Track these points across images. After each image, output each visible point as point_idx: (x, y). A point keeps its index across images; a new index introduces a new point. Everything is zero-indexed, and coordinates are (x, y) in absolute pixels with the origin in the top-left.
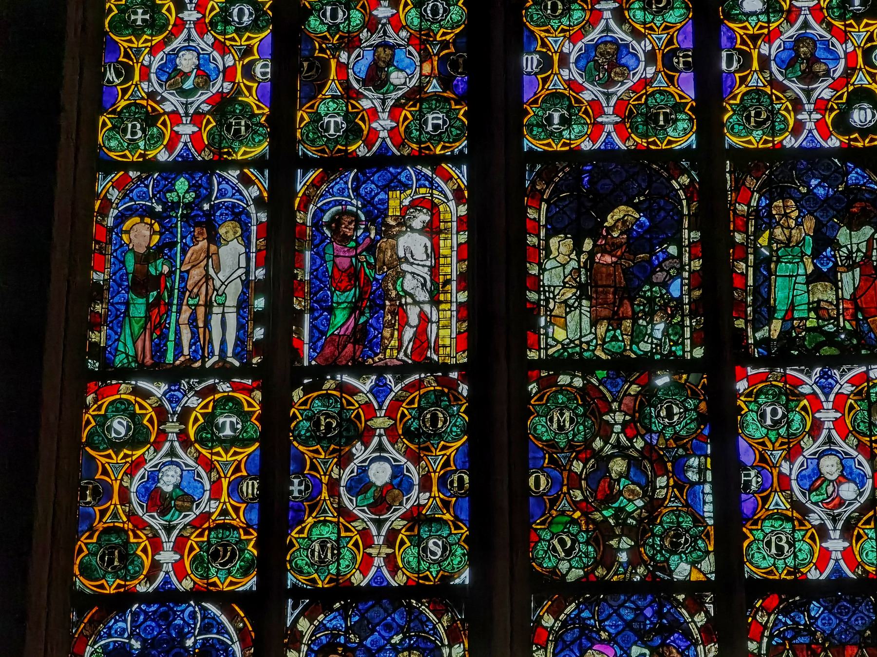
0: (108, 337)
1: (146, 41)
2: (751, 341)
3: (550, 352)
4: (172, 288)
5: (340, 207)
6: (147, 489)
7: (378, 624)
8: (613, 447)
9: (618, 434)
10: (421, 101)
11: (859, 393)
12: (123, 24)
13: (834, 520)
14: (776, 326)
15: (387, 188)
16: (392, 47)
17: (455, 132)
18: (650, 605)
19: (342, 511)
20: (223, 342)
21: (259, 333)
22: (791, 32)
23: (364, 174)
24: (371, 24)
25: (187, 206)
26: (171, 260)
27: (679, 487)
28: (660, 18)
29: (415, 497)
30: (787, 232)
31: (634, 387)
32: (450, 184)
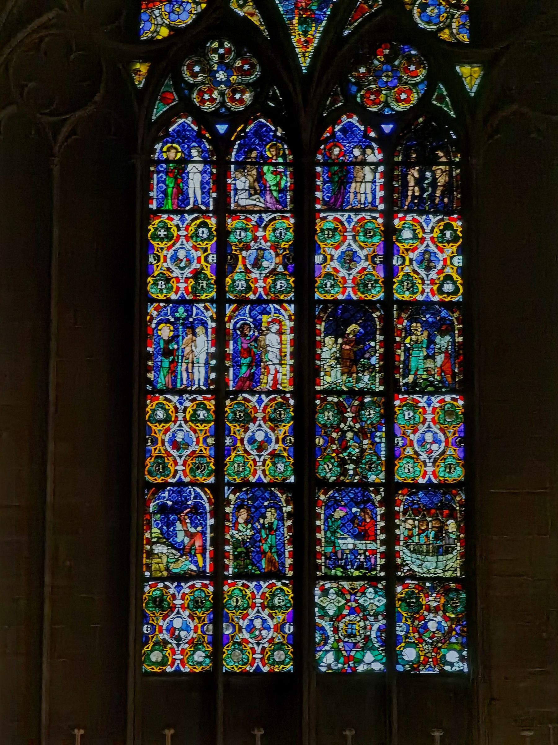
0: (155, 376)
1: (166, 244)
2: (401, 384)
3: (325, 386)
5: (243, 322)
6: (171, 440)
7: (259, 497)
9: (350, 422)
10: (275, 275)
11: (441, 407)
12: (155, 237)
13: (430, 458)
14: (411, 378)
15: (262, 313)
16: (264, 250)
17: (289, 289)
18: (360, 492)
19: (246, 451)
20: (199, 379)
21: (213, 376)
22: (422, 248)
23: (253, 307)
24: (255, 239)
25: (183, 319)
26: (178, 343)
27: (372, 444)
28: (370, 240)
30: (417, 337)
31: (356, 402)
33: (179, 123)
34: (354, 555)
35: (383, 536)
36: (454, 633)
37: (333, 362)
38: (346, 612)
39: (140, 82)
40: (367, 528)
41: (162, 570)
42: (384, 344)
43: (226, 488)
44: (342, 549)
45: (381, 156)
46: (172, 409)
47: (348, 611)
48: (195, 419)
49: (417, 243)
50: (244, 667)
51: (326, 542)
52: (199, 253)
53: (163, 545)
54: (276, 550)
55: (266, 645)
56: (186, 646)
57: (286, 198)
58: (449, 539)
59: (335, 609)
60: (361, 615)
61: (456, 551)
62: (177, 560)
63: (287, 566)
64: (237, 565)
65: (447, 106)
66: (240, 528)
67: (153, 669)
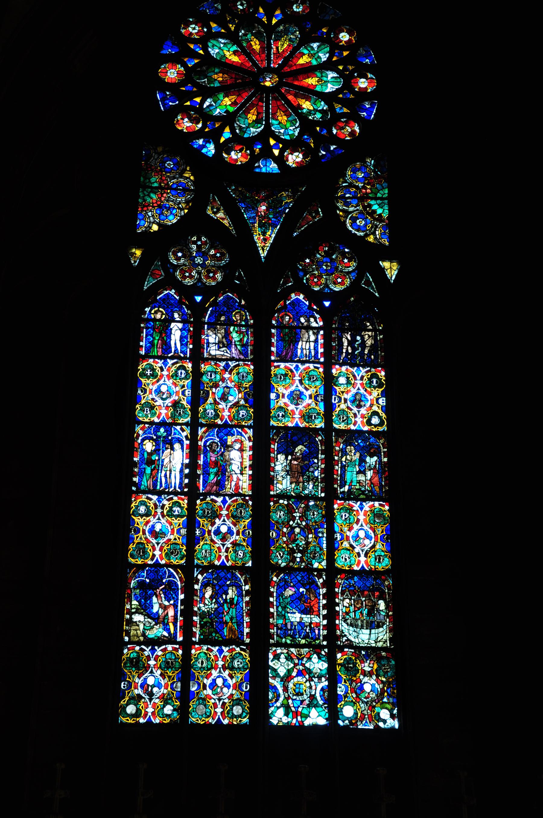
0: (139, 480)
1: (151, 381)
2: (339, 492)
3: (277, 492)
4: (159, 464)
5: (212, 441)
8: (296, 524)
9: (297, 520)
10: (238, 406)
11: (371, 511)
12: (143, 375)
13: (362, 551)
14: (346, 488)
15: (227, 435)
19: (212, 540)
20: (175, 483)
21: (186, 481)
22: (354, 391)
23: (220, 430)
24: (223, 380)
25: (164, 437)
26: (159, 455)
28: (313, 384)
29: (235, 537)
31: (303, 505)
32: (247, 435)
33: (164, 293)
34: (302, 627)
35: (325, 612)
36: (386, 694)
37: (283, 473)
38: (294, 674)
39: (135, 262)
40: (312, 604)
41: (139, 636)
42: (324, 461)
43: (196, 569)
44: (291, 622)
45: (321, 324)
46: (152, 505)
47: (296, 673)
48: (170, 513)
49: (350, 387)
50: (207, 720)
51: (277, 615)
52: (178, 389)
53: (140, 615)
54: (236, 621)
55: (226, 701)
56: (157, 701)
57: (248, 351)
58: (380, 616)
59: (285, 671)
60: (307, 676)
61: (386, 625)
62: (152, 628)
63: (245, 634)
64: (203, 633)
65: (373, 288)
66: (207, 602)
67: (128, 720)
